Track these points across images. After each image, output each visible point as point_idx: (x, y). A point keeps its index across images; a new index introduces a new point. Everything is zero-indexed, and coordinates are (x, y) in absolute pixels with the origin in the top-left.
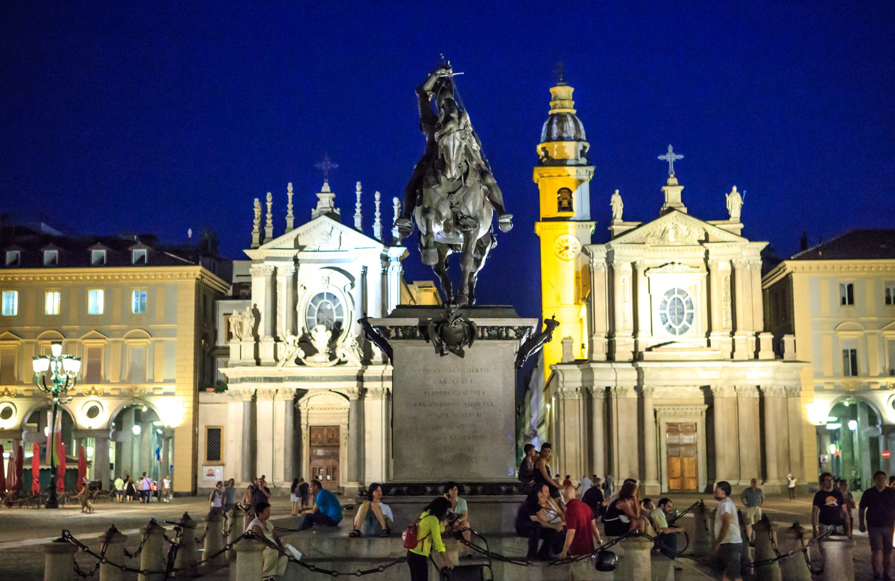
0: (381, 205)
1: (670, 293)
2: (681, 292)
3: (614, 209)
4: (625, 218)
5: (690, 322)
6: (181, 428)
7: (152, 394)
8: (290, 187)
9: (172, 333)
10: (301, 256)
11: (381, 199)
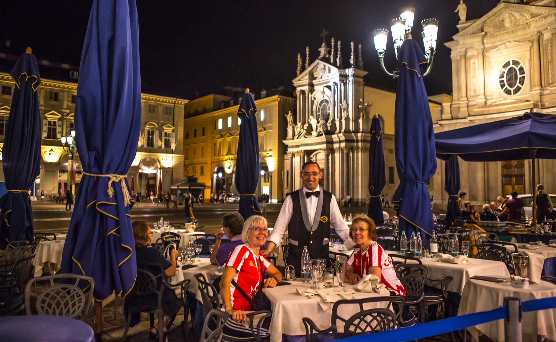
0: (341, 48)
1: (507, 64)
2: (516, 63)
3: (460, 14)
4: (470, 17)
5: (522, 85)
6: (274, 171)
7: (266, 156)
8: (307, 49)
9: (271, 128)
10: (314, 82)
11: (341, 45)
